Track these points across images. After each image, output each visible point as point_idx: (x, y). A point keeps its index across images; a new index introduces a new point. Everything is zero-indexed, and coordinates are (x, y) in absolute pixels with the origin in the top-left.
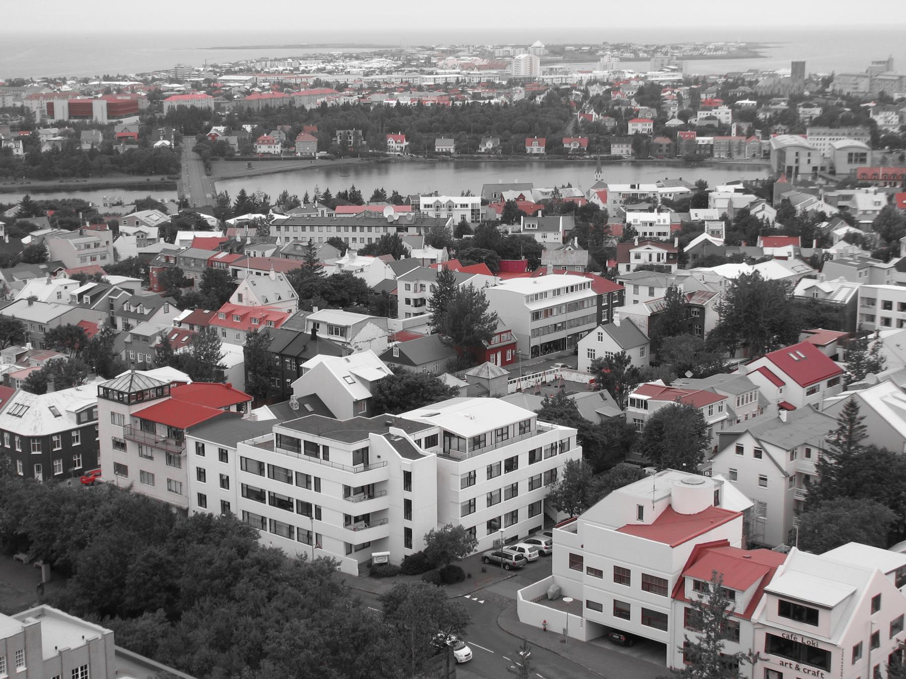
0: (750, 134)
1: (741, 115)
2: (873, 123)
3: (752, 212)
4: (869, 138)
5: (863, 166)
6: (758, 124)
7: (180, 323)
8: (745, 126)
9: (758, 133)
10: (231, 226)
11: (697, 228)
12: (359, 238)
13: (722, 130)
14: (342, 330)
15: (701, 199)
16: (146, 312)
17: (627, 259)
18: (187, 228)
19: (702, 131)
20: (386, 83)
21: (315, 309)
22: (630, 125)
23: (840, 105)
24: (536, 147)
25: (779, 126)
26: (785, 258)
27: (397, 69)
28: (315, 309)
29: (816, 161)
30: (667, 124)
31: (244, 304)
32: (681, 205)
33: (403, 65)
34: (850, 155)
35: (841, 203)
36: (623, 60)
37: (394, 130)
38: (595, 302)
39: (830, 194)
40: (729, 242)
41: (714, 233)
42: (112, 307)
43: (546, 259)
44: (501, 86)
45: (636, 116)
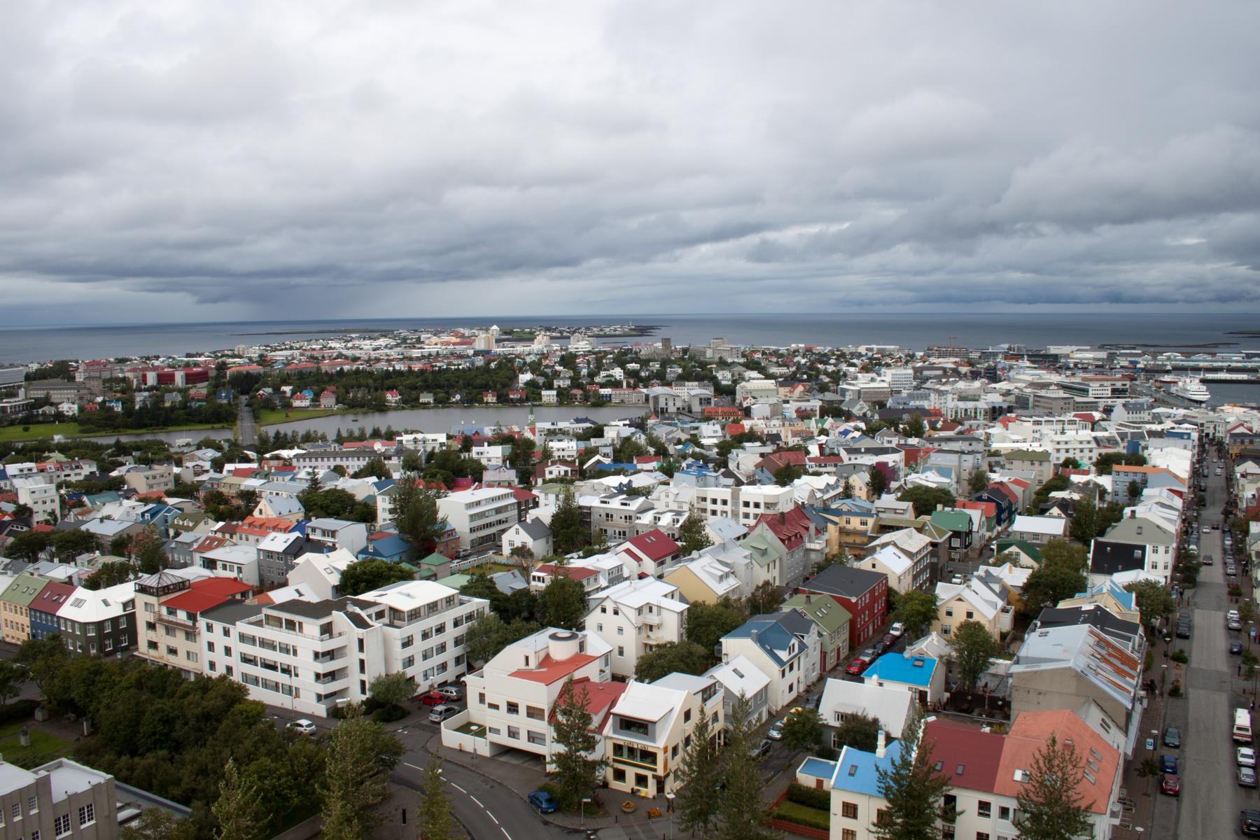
0: (635, 387)
1: (629, 374)
2: (715, 377)
3: (634, 439)
4: (712, 389)
5: (709, 407)
6: (641, 380)
7: (216, 532)
8: (632, 381)
9: (641, 385)
10: (267, 459)
11: (593, 452)
12: (354, 465)
13: (616, 384)
14: (333, 534)
15: (598, 432)
16: (191, 524)
17: (543, 475)
18: (231, 461)
19: (603, 386)
20: (387, 355)
21: (313, 519)
22: (555, 381)
23: (694, 367)
24: (490, 398)
25: (653, 382)
26: (651, 471)
27: (397, 345)
28: (313, 519)
29: (679, 404)
30: (580, 381)
31: (263, 516)
32: (583, 437)
33: (402, 343)
34: (701, 399)
35: (692, 432)
36: (552, 338)
37: (390, 389)
38: (516, 506)
39: (685, 426)
40: (616, 460)
41: (606, 455)
42: (166, 521)
43: (487, 476)
44: (468, 357)
45: (559, 376)
